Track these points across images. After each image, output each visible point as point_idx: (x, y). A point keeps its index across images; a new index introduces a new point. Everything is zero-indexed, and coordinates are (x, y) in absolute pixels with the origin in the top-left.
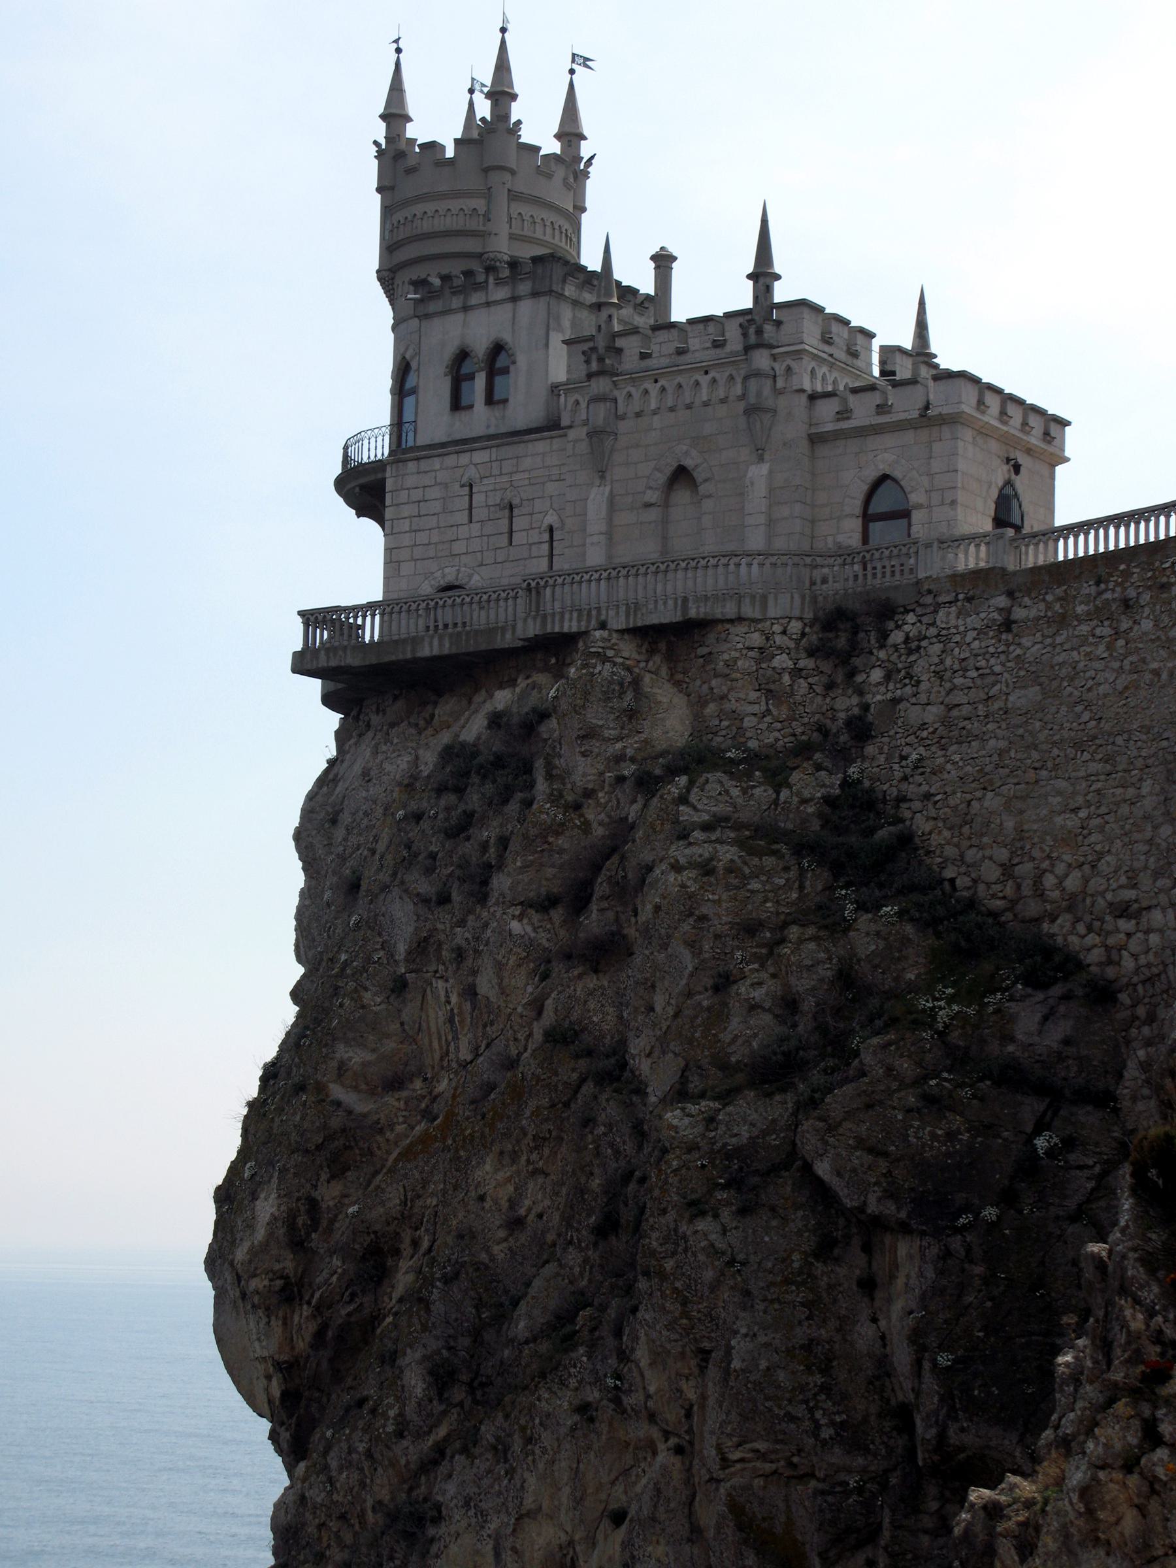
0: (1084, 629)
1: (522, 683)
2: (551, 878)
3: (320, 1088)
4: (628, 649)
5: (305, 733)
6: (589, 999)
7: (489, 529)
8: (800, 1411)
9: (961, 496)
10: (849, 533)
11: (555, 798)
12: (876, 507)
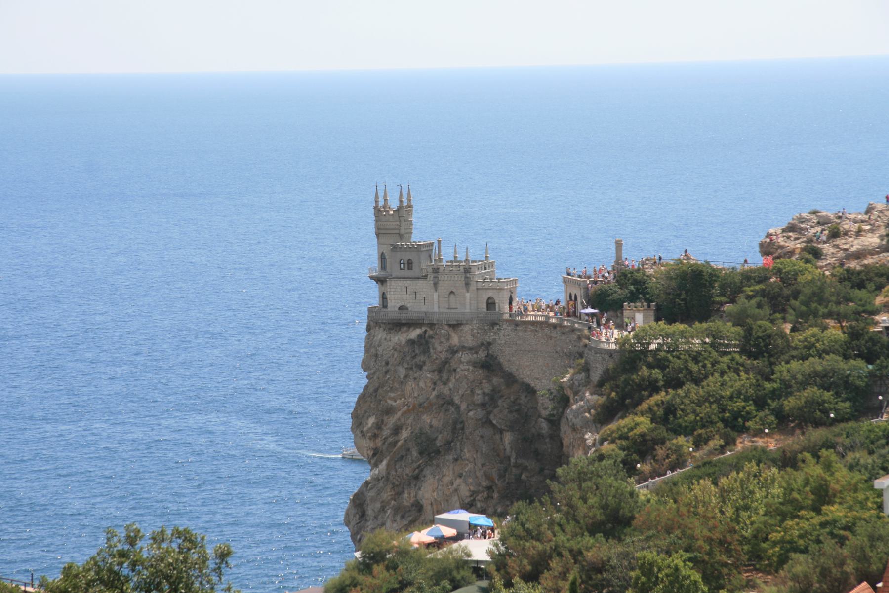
1: (424, 329)
2: (434, 367)
4: (446, 327)
12: (490, 301)
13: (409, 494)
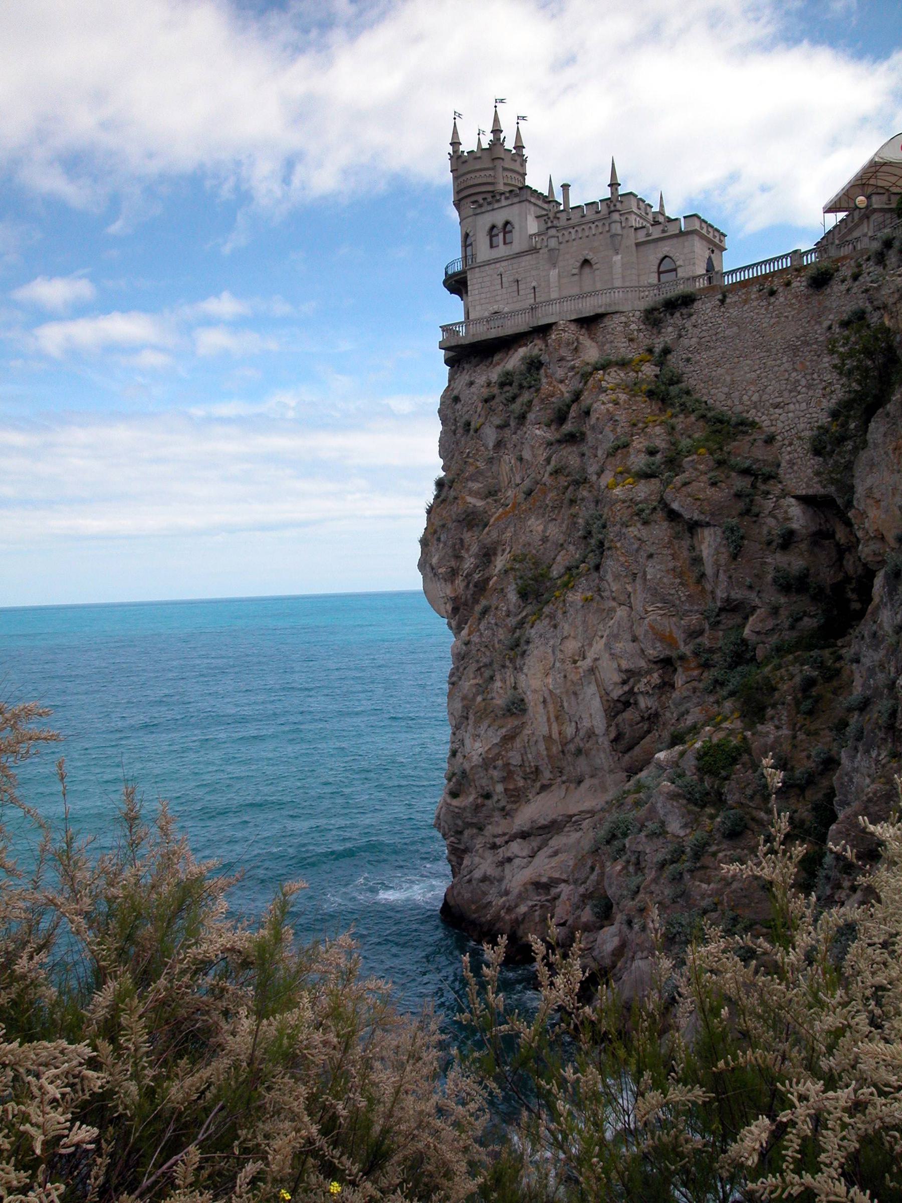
0: (755, 303)
3: (463, 498)
4: (573, 327)
5: (438, 375)
6: (570, 456)
7: (510, 290)
8: (673, 592)
9: (697, 261)
10: (653, 279)
11: (550, 384)
13: (504, 680)
